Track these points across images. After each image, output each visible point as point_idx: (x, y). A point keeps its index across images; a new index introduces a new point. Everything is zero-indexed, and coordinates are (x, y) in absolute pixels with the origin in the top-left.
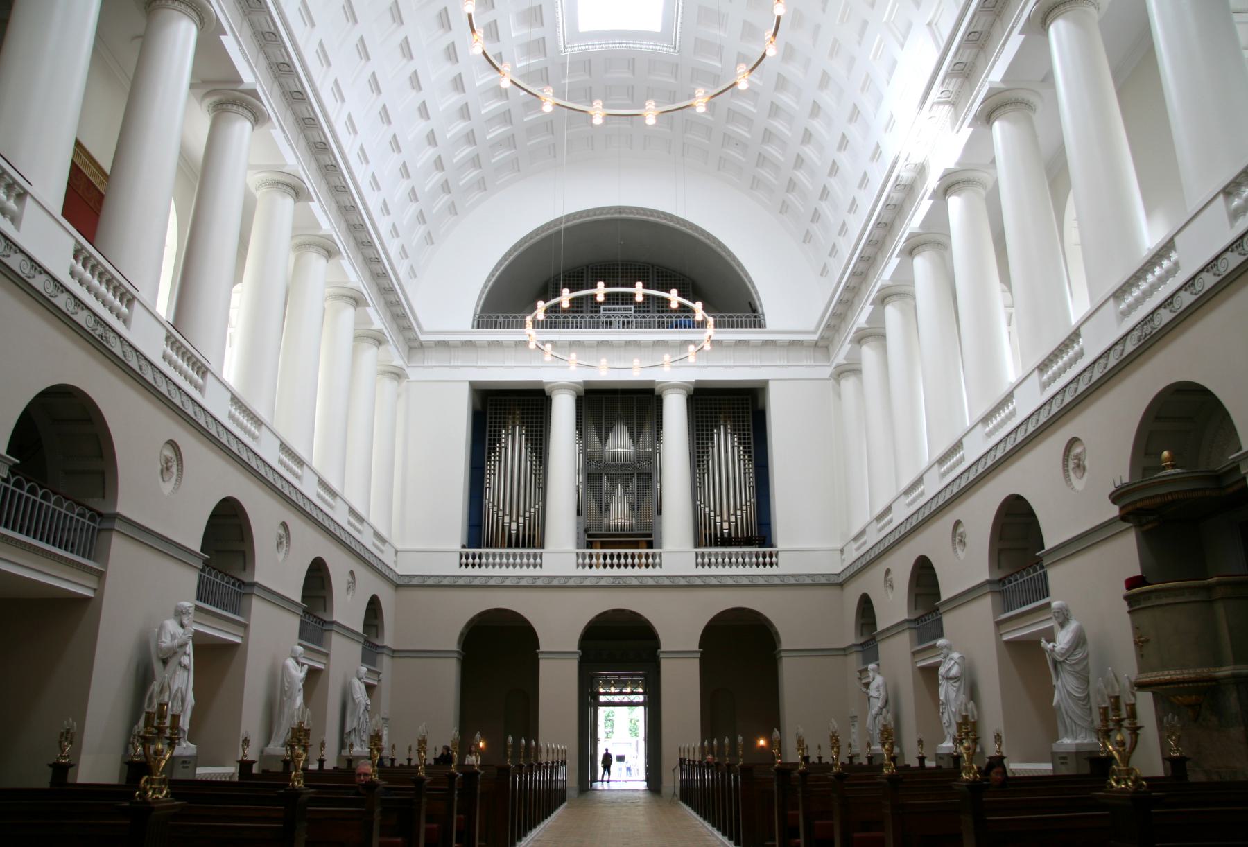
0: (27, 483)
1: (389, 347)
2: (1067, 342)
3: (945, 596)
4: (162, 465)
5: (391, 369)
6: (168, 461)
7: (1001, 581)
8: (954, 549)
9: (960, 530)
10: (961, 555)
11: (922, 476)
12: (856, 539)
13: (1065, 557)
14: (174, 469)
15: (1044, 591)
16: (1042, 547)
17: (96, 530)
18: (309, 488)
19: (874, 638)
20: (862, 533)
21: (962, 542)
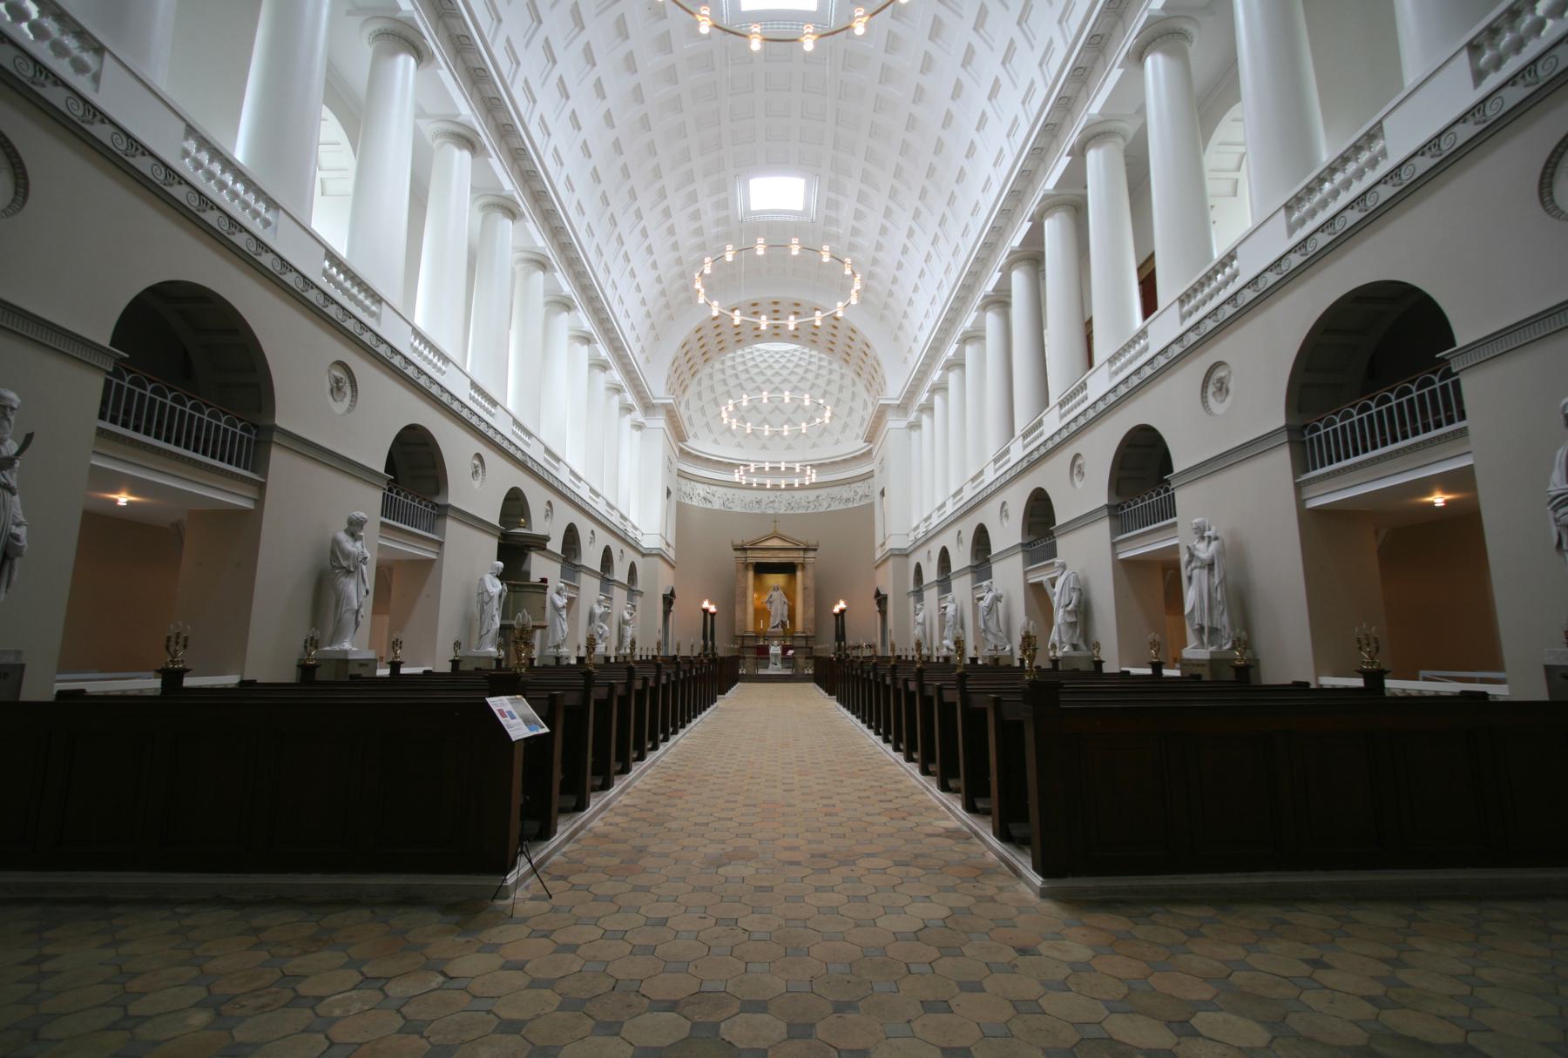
0: (170, 393)
1: (612, 372)
2: (1135, 339)
3: (994, 551)
4: (331, 385)
5: (581, 334)
6: (338, 381)
7: (1119, 507)
8: (1002, 523)
9: (1006, 508)
10: (1079, 484)
11: (983, 470)
12: (940, 508)
13: (1258, 454)
14: (347, 389)
15: (1169, 510)
16: (1171, 470)
17: (253, 442)
18: (565, 477)
19: (949, 577)
20: (943, 505)
21: (1007, 516)
